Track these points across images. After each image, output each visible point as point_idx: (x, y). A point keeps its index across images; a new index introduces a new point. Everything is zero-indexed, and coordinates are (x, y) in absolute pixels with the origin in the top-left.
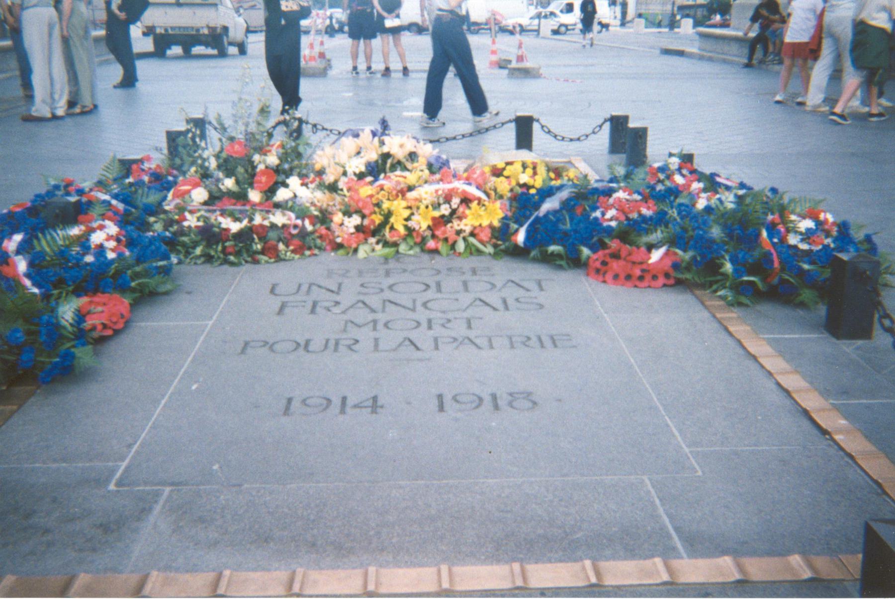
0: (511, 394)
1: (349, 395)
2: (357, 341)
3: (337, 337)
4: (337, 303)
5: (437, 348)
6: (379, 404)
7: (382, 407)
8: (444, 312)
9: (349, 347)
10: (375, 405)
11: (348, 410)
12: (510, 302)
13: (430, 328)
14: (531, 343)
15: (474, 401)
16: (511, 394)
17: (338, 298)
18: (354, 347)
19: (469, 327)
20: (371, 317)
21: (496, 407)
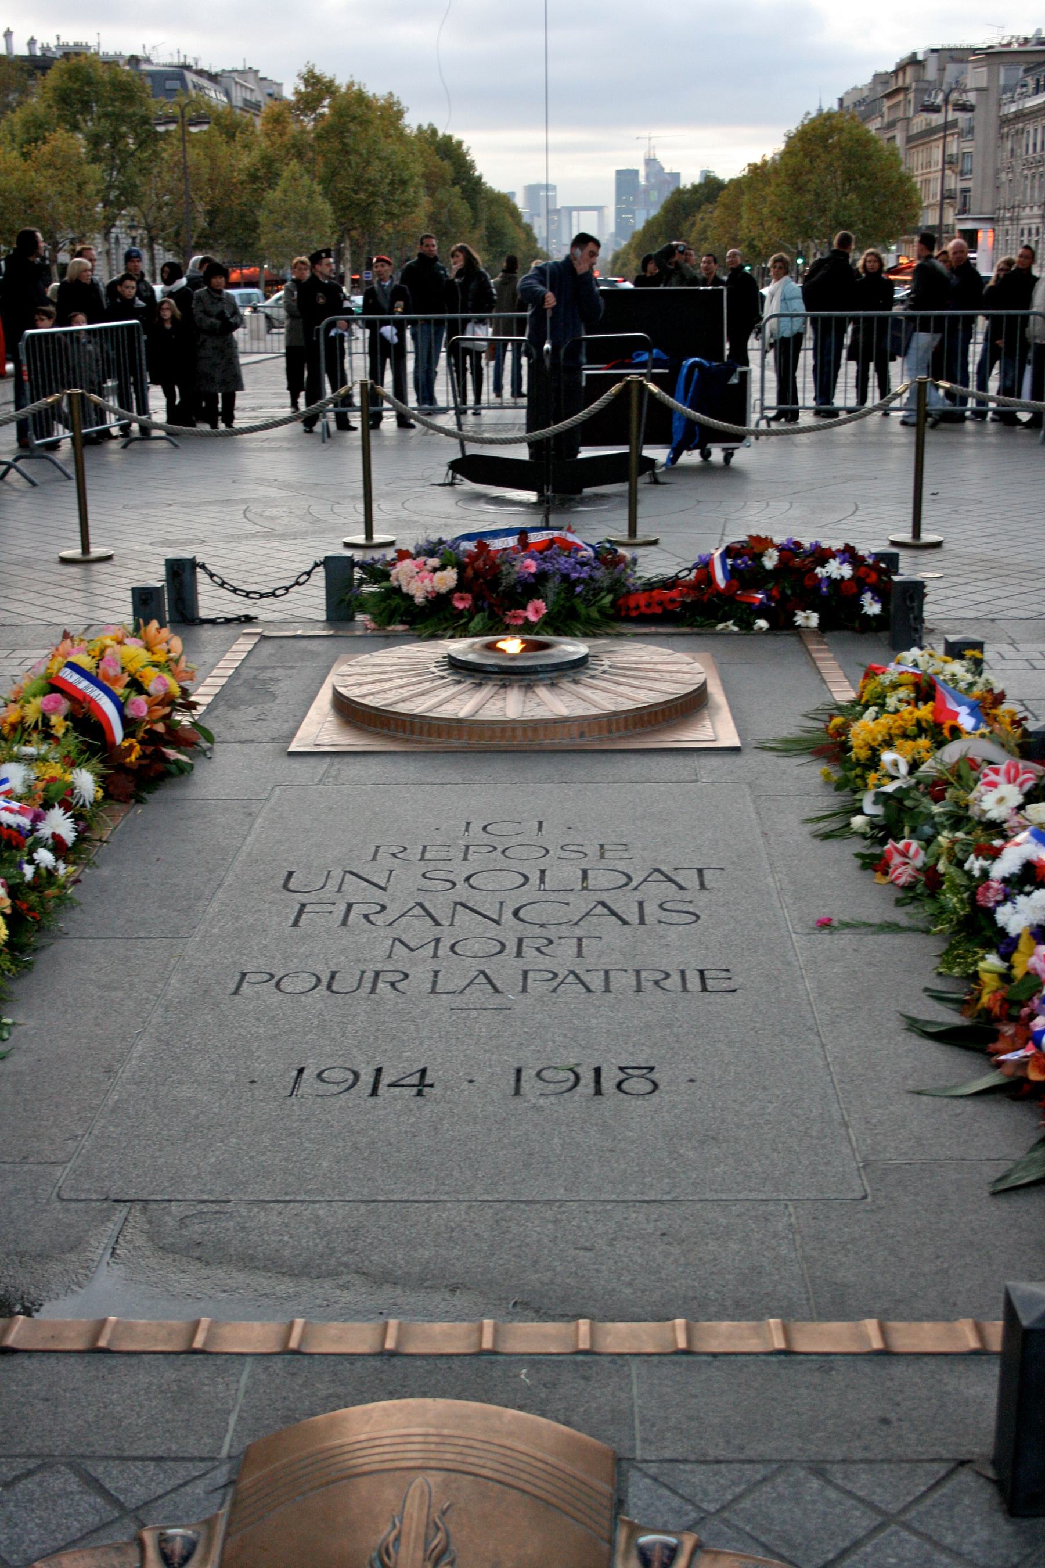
0: (622, 1069)
1: (385, 1066)
2: (406, 976)
3: (379, 967)
4: (384, 908)
5: (524, 990)
6: (427, 1081)
7: (431, 1086)
8: (542, 926)
9: (393, 984)
10: (422, 1083)
11: (382, 1089)
12: (650, 909)
13: (519, 954)
14: (667, 984)
15: (568, 1080)
16: (622, 1069)
17: (385, 901)
18: (399, 986)
19: (580, 954)
20: (434, 932)
21: (598, 1092)
